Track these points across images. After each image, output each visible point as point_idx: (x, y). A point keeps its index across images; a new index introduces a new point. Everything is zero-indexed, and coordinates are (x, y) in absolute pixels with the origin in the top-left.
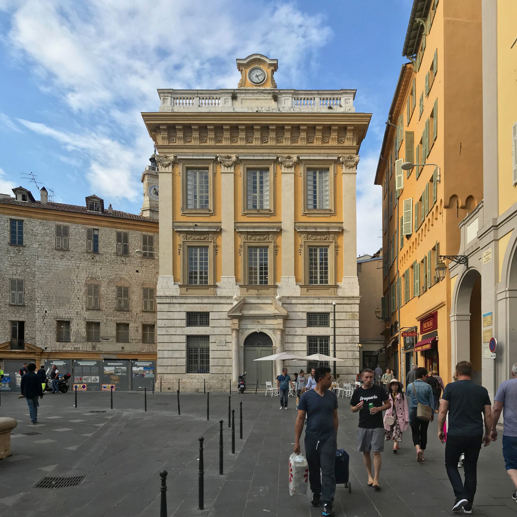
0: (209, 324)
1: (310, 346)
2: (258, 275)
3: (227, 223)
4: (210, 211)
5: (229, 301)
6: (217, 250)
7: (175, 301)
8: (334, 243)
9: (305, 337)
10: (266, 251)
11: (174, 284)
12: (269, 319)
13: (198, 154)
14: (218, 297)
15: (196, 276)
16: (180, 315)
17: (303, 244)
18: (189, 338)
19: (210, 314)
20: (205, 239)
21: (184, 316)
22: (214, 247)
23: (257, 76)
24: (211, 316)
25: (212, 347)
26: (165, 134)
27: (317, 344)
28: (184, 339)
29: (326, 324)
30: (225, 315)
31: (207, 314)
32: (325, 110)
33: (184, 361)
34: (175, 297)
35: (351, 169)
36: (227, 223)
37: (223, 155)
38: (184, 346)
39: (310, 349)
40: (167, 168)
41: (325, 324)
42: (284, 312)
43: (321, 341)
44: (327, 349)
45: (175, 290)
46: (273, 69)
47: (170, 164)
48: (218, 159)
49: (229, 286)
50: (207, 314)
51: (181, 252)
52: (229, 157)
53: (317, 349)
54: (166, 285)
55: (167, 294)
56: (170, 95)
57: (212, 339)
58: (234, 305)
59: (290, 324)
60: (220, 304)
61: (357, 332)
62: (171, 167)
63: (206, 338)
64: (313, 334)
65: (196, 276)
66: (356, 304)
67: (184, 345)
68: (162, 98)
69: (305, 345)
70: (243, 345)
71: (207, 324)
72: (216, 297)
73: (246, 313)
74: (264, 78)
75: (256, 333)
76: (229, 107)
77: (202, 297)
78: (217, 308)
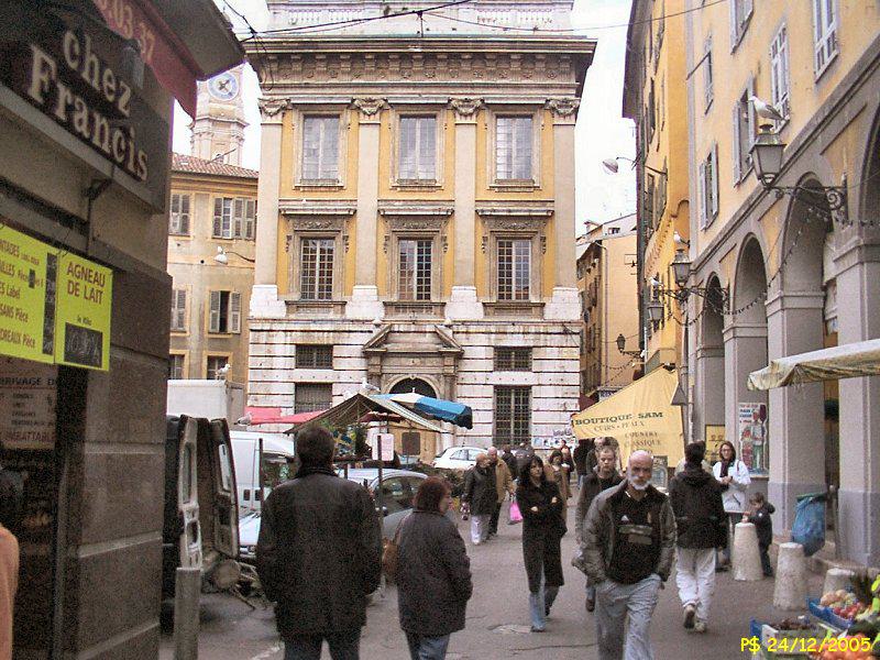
2: (418, 289)
10: (429, 245)
15: (316, 284)
16: (284, 348)
18: (299, 386)
21: (291, 350)
24: (336, 351)
27: (510, 399)
28: (291, 389)
30: (357, 351)
31: (330, 348)
34: (279, 321)
37: (364, 97)
40: (274, 118)
43: (516, 394)
45: (279, 311)
49: (365, 303)
55: (267, 315)
58: (374, 335)
59: (466, 365)
60: (350, 331)
61: (576, 379)
62: (280, 115)
64: (503, 383)
65: (316, 284)
67: (293, 398)
71: (329, 365)
73: (390, 347)
78: (345, 338)
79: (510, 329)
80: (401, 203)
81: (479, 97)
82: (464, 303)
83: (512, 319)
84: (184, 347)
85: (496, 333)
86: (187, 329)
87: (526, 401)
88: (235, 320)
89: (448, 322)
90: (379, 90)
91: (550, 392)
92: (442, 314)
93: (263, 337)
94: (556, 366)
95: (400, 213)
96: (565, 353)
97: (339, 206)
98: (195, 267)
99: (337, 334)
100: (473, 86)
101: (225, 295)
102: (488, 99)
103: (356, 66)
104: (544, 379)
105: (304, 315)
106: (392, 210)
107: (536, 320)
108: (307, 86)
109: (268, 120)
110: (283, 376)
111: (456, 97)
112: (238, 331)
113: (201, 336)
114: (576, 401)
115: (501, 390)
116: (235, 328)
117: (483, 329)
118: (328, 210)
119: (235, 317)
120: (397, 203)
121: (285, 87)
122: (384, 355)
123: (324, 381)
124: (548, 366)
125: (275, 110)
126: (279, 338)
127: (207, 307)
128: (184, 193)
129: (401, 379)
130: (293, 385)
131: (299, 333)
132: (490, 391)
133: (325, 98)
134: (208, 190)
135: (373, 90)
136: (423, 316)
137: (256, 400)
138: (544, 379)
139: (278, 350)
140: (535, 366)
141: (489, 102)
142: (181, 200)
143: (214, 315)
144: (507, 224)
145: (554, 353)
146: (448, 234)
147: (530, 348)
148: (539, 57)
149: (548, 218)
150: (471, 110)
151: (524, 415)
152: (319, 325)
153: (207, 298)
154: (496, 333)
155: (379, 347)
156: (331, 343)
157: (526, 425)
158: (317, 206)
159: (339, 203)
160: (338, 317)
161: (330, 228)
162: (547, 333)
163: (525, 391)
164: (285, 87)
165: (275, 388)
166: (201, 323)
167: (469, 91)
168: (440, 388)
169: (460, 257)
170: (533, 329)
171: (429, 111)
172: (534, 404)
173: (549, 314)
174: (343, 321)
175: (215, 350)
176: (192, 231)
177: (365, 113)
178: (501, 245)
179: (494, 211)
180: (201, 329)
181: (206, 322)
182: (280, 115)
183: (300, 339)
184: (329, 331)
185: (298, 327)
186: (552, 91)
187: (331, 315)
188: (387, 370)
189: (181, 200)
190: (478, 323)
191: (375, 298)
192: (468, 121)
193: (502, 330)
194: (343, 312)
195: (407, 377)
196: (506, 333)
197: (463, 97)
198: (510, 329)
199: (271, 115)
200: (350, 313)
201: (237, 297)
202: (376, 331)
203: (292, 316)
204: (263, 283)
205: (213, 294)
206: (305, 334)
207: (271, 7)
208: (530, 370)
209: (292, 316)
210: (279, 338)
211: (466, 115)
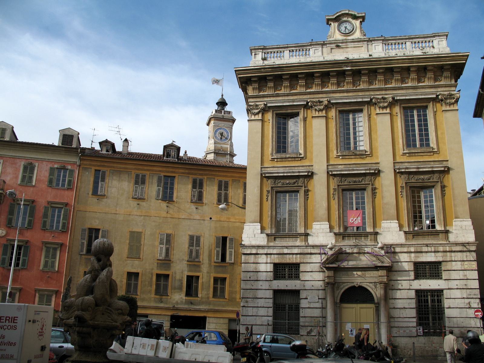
0: (299, 277)
1: (419, 302)
3: (319, 167)
4: (300, 154)
6: (308, 195)
7: (261, 251)
8: (439, 183)
9: (414, 291)
11: (261, 233)
12: (369, 271)
13: (289, 101)
14: (310, 246)
16: (265, 267)
17: (404, 185)
18: (277, 293)
20: (294, 183)
21: (270, 268)
22: (305, 191)
23: (346, 27)
24: (302, 268)
25: (304, 304)
26: (256, 85)
27: (427, 300)
28: (270, 294)
30: (317, 267)
31: (297, 266)
32: (417, 52)
34: (263, 247)
35: (452, 106)
36: (319, 167)
38: (270, 303)
39: (419, 306)
40: (257, 116)
41: (436, 276)
42: (387, 262)
43: (432, 296)
44: (441, 305)
45: (262, 240)
46: (361, 20)
47: (259, 112)
48: (309, 104)
50: (297, 266)
51: (270, 198)
52: (321, 102)
53: (428, 305)
54: (252, 234)
55: (254, 243)
56: (261, 51)
57: (303, 295)
60: (311, 254)
61: (476, 284)
62: (260, 115)
63: (296, 293)
64: (422, 287)
66: (472, 251)
67: (271, 301)
68: (253, 54)
69: (414, 301)
70: (338, 301)
71: (297, 277)
72: (308, 246)
74: (353, 29)
75: (354, 287)
76: (319, 56)
77: (292, 246)
78: (308, 259)
79: (425, 249)
80: (343, 166)
81: (391, 96)
82: (391, 233)
83: (426, 242)
84: (200, 271)
85: (415, 252)
86: (201, 260)
87: (440, 301)
88: (231, 255)
89: (380, 245)
90: (324, 95)
91: (457, 294)
92: (376, 240)
93: (252, 259)
94: (461, 275)
95: (343, 173)
96: (466, 265)
97: (301, 169)
98: (206, 222)
99: (302, 256)
100: (386, 89)
101: (224, 239)
102: (397, 96)
103: (309, 82)
104: (453, 284)
105: (278, 243)
106: (337, 171)
107: (443, 242)
108: (278, 95)
109: (253, 117)
110: (265, 285)
111: (376, 96)
112: (233, 261)
113: (210, 264)
114: (478, 301)
116: (231, 259)
117: (405, 250)
118: (293, 172)
119: (231, 252)
120: (340, 167)
121: (264, 96)
122: (337, 270)
123: (294, 288)
124: (454, 275)
125: (256, 111)
126: (263, 259)
127: (214, 246)
128: (200, 177)
129: (346, 287)
130: (271, 292)
131: (276, 256)
132: (413, 294)
133: (289, 102)
134: (214, 175)
135: (321, 96)
136: (363, 241)
137: (247, 302)
138: (453, 284)
139: (262, 268)
140: (445, 275)
141: (398, 98)
142: (198, 182)
143: (218, 252)
144: (416, 177)
145: (458, 265)
146: (377, 184)
147: (440, 263)
148: (430, 68)
149: (447, 171)
150: (386, 104)
151: (439, 312)
152: (290, 250)
153: (213, 240)
154: (415, 252)
155: (332, 263)
156: (298, 261)
158: (287, 170)
159: (301, 168)
160: (303, 244)
161: (296, 185)
162: (451, 252)
164: (264, 96)
165: (260, 294)
166: (210, 256)
167: (384, 92)
168: (377, 292)
169: (385, 201)
170: (441, 249)
171: (357, 108)
172: (446, 303)
173: (452, 238)
174: (306, 246)
175: (218, 273)
176: (205, 200)
177: (316, 110)
178: (413, 192)
179: (407, 168)
180: (210, 260)
181: (213, 255)
182: (260, 115)
183: (277, 259)
184: (297, 254)
185: (275, 251)
186: (439, 89)
187: (298, 243)
188: (338, 279)
189: (198, 182)
190: (402, 245)
191: (329, 230)
192: (385, 111)
193: (419, 250)
194: (306, 240)
195: (352, 285)
196: (421, 252)
197: (380, 97)
198: (425, 249)
199: (255, 114)
200: (311, 241)
201: (231, 240)
202: (330, 253)
203: (272, 244)
204: (250, 222)
205: (217, 238)
206: (280, 256)
207: (253, 51)
208: (441, 278)
209: (272, 244)
210: (263, 259)
211: (383, 108)
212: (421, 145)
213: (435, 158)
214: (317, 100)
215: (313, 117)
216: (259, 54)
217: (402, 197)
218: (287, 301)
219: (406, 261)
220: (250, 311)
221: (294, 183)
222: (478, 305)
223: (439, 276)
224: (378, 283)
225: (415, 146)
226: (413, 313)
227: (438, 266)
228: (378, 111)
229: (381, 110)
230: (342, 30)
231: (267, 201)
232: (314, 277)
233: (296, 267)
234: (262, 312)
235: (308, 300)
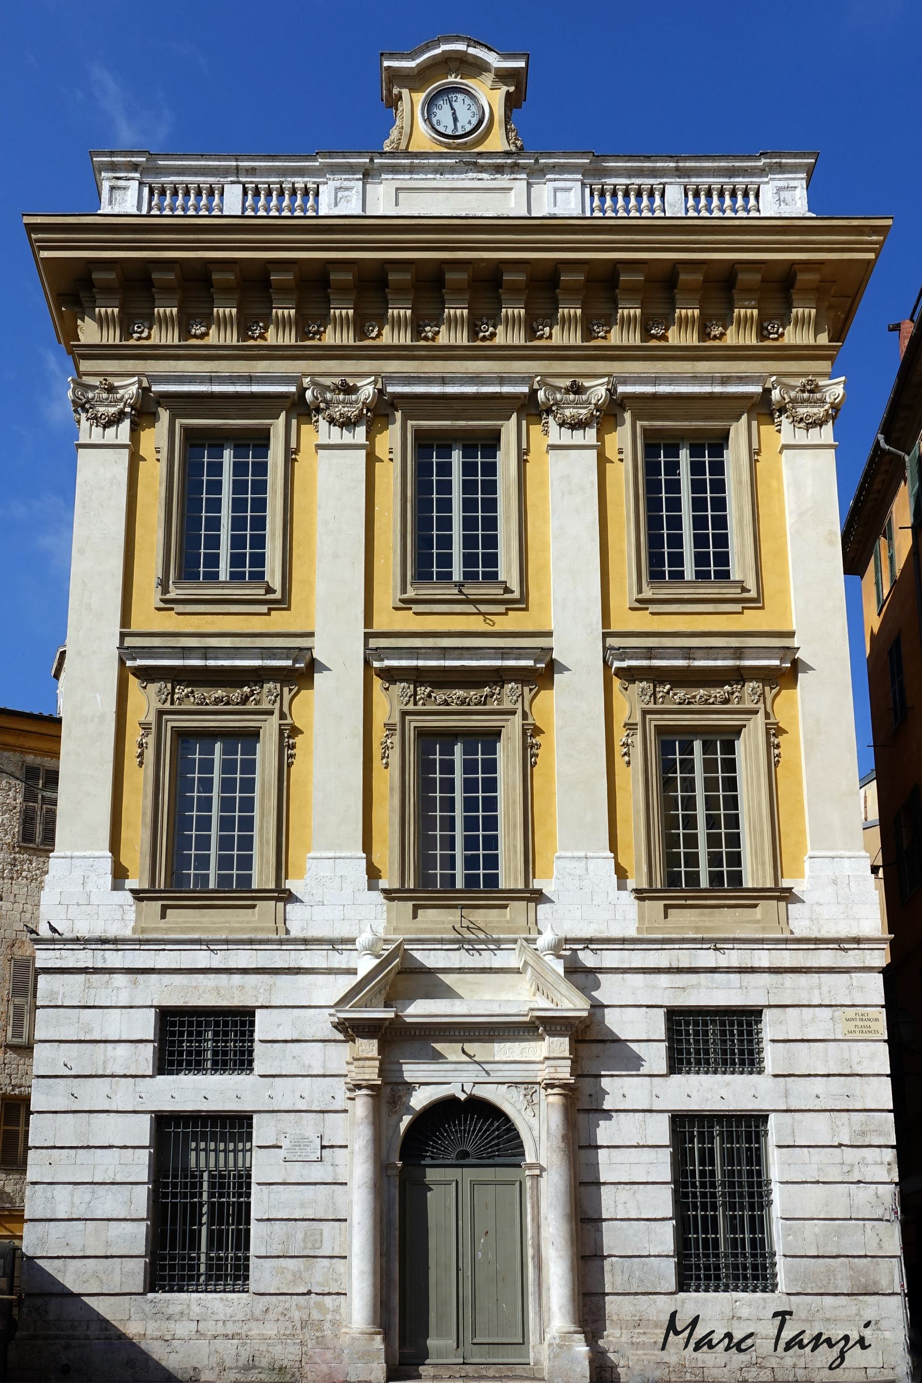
0: (251, 1062)
4: (269, 590)
5: (338, 960)
8: (761, 716)
9: (664, 1122)
14: (295, 941)
17: (638, 719)
19: (260, 1017)
20: (245, 700)
21: (145, 1025)
22: (281, 732)
25: (263, 1166)
29: (749, 1060)
33: (135, 1237)
35: (814, 431)
38: (139, 1166)
44: (759, 1173)
51: (150, 754)
57: (262, 1131)
60: (298, 971)
61: (882, 1093)
63: (235, 1126)
64: (694, 1105)
72: (286, 942)
74: (480, 122)
75: (451, 1101)
77: (227, 942)
87: (756, 1158)
91: (818, 1128)
104: (804, 1093)
115: (684, 1124)
124: (807, 1058)
132: (660, 1129)
138: (804, 1093)
151: (753, 1193)
157: (759, 1224)
163: (748, 1127)
172: (776, 1166)
174: (281, 942)
211: (577, 425)
212: (702, 576)
213: (751, 620)
214: (337, 381)
215: (319, 447)
216: (125, 188)
217: (628, 763)
218: (204, 1159)
219: (635, 1012)
220: (63, 1202)
221: (245, 700)
222: (889, 1171)
223: (752, 1063)
224: (537, 1087)
225: (678, 576)
226: (663, 1202)
227: (749, 1024)
228: (553, 439)
229: (565, 431)
230: (439, 122)
231: (141, 763)
232: (307, 1063)
233: (243, 1024)
234: (109, 1203)
235: (282, 1153)
